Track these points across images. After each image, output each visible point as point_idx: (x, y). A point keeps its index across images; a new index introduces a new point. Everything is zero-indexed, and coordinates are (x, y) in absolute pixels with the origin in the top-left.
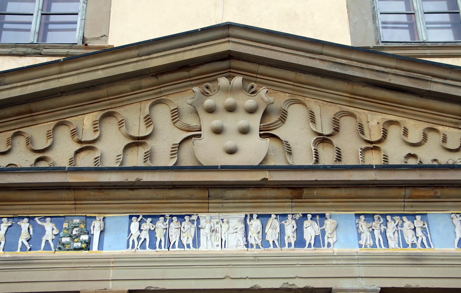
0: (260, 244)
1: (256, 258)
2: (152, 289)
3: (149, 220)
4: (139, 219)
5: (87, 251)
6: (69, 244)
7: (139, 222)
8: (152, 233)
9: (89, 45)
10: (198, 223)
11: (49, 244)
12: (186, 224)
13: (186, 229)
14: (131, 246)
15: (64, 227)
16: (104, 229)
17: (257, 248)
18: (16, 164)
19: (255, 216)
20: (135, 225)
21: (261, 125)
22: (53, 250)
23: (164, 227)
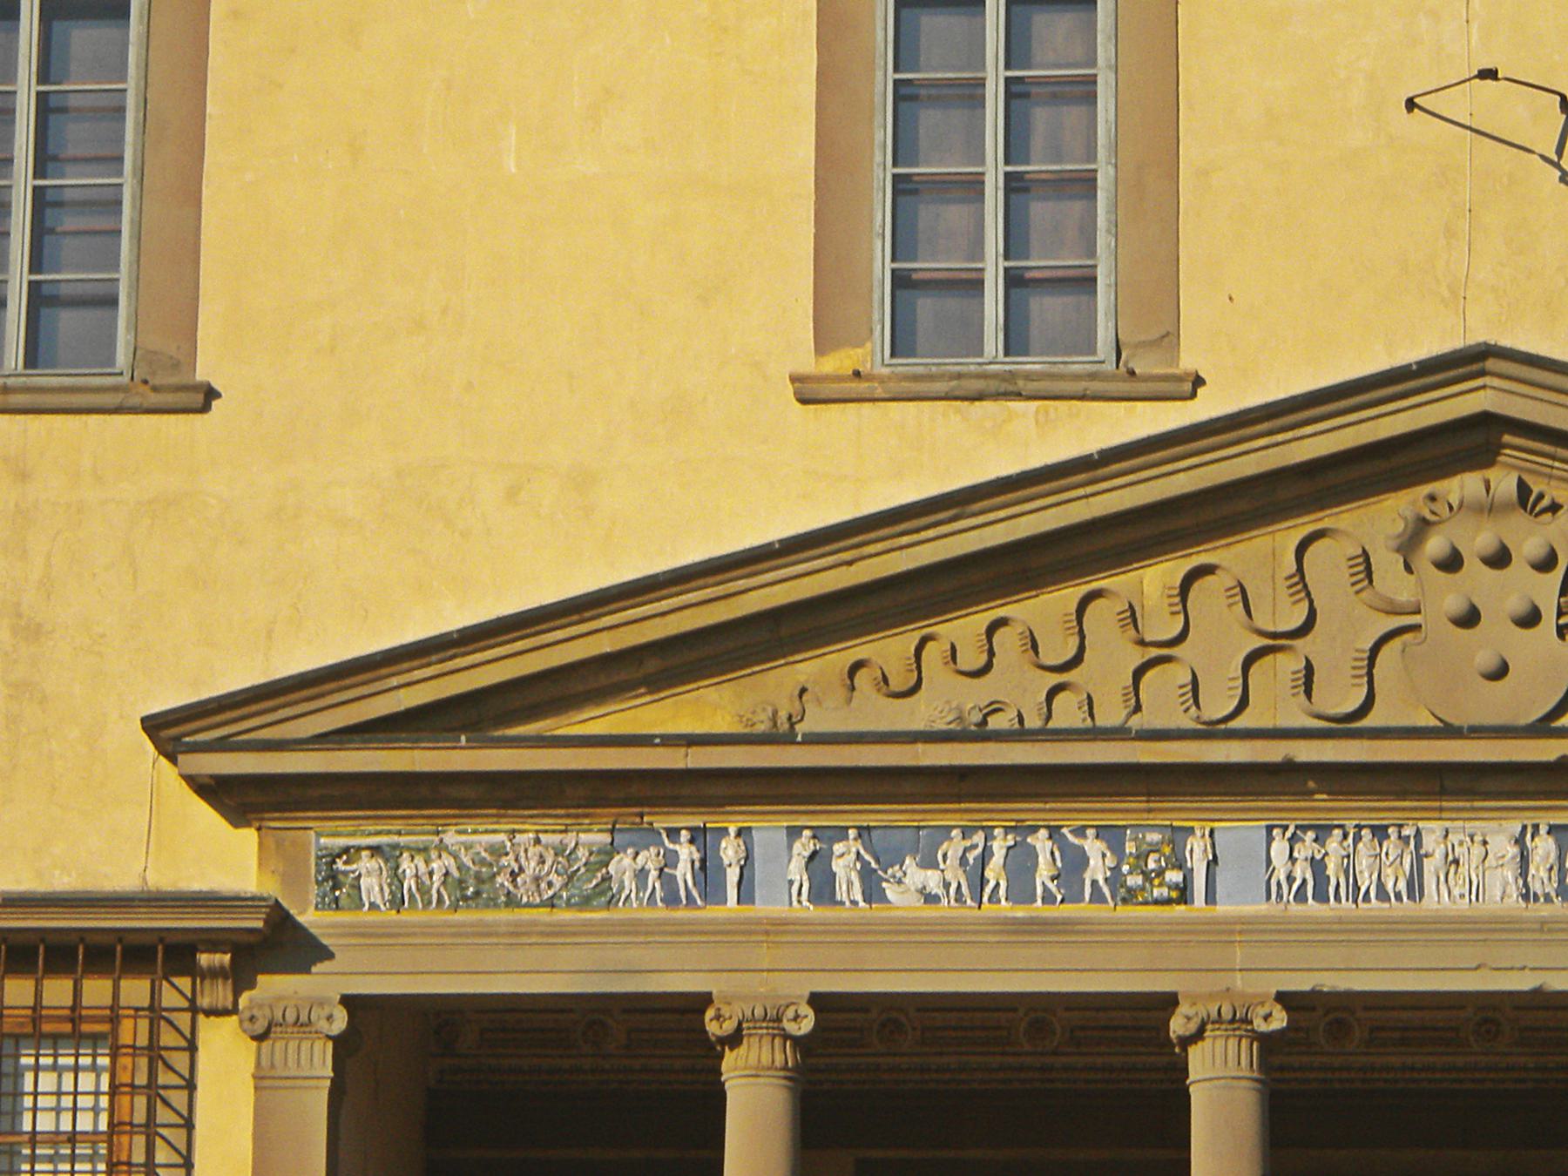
0: (1553, 894)
1: (1543, 925)
2: (1325, 989)
3: (1311, 835)
4: (1288, 834)
5: (1182, 907)
6: (1143, 889)
7: (1289, 840)
8: (1318, 866)
9: (1137, 371)
10: (1418, 845)
11: (1100, 889)
12: (1391, 845)
13: (1391, 858)
14: (1274, 896)
15: (1127, 851)
16: (1215, 856)
17: (1545, 900)
18: (1007, 700)
19: (1543, 830)
20: (1279, 848)
21: (1562, 600)
22: (1111, 904)
23: (1345, 853)
